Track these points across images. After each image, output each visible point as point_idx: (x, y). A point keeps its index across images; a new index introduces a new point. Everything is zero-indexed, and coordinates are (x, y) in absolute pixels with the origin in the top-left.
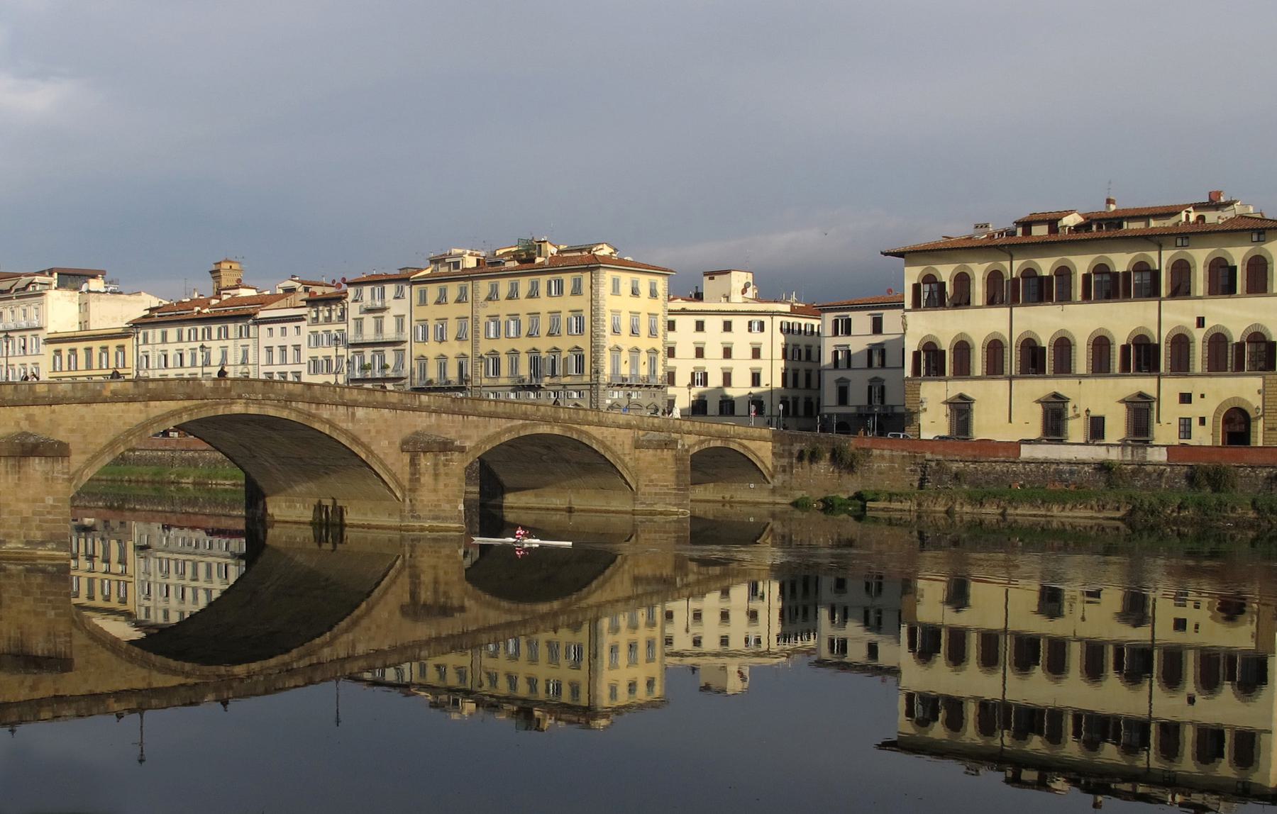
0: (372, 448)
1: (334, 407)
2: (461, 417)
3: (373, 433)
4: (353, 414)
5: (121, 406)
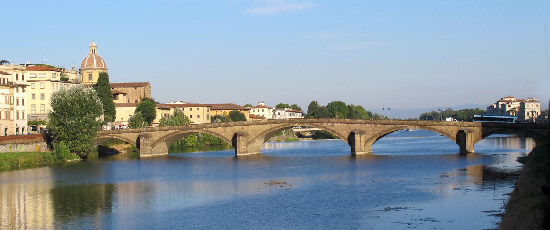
0: (340, 133)
1: (327, 124)
2: (374, 125)
3: (340, 130)
4: (333, 125)
5: (264, 125)
